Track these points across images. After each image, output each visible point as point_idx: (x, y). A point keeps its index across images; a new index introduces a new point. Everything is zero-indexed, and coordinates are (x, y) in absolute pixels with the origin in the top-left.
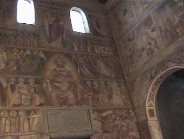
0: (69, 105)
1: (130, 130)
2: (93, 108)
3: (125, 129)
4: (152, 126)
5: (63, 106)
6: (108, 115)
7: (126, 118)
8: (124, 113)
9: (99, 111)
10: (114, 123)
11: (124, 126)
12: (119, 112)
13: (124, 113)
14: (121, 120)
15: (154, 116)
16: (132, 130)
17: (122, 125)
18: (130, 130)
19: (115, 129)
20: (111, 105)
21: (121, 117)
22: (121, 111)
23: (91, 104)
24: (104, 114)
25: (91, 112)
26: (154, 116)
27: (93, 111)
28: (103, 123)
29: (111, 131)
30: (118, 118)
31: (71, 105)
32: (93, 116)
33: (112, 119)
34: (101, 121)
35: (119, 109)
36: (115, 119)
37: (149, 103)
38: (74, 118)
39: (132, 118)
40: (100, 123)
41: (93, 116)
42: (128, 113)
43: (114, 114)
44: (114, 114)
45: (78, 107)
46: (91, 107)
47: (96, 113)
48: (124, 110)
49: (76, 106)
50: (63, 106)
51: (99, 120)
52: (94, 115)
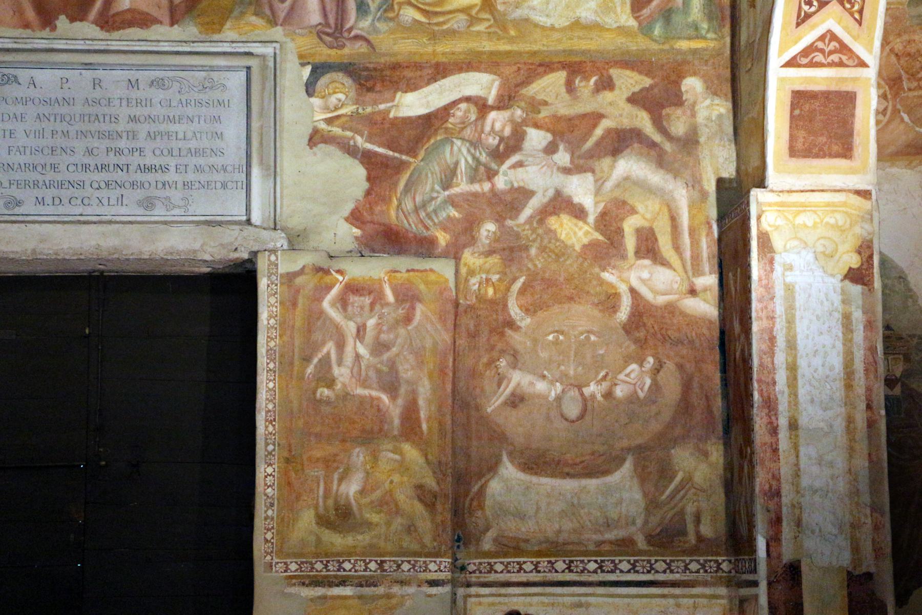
0: (108, 22)
1: (630, 243)
2: (326, 54)
3: (575, 234)
4: (777, 241)
5: (62, 22)
6: (446, 111)
7: (621, 141)
8: (617, 108)
9: (375, 77)
10: (491, 175)
11: (579, 213)
12: (570, 87)
13: (617, 108)
14: (563, 157)
15: (846, 152)
16: (648, 247)
17: (560, 204)
18: (630, 243)
19: (489, 228)
20: (501, 24)
21: (567, 131)
22: (585, 86)
23: (315, 18)
24: (412, 104)
25: (295, 75)
26: (846, 152)
27: (319, 70)
28: (381, 172)
29: (443, 239)
30: (536, 138)
31: (142, 20)
32: (302, 111)
33: (475, 144)
34: (367, 159)
35: (575, 67)
36: (512, 144)
37: (809, 35)
38: (133, 119)
39: (690, 142)
40: (360, 172)
41: (301, 112)
42: (660, 99)
43: (505, 101)
44: (503, 103)
45: (188, 30)
46: (308, 43)
47: (340, 95)
48: (614, 72)
49: (176, 32)
50: (62, 22)
51: (351, 151)
52: (316, 101)
